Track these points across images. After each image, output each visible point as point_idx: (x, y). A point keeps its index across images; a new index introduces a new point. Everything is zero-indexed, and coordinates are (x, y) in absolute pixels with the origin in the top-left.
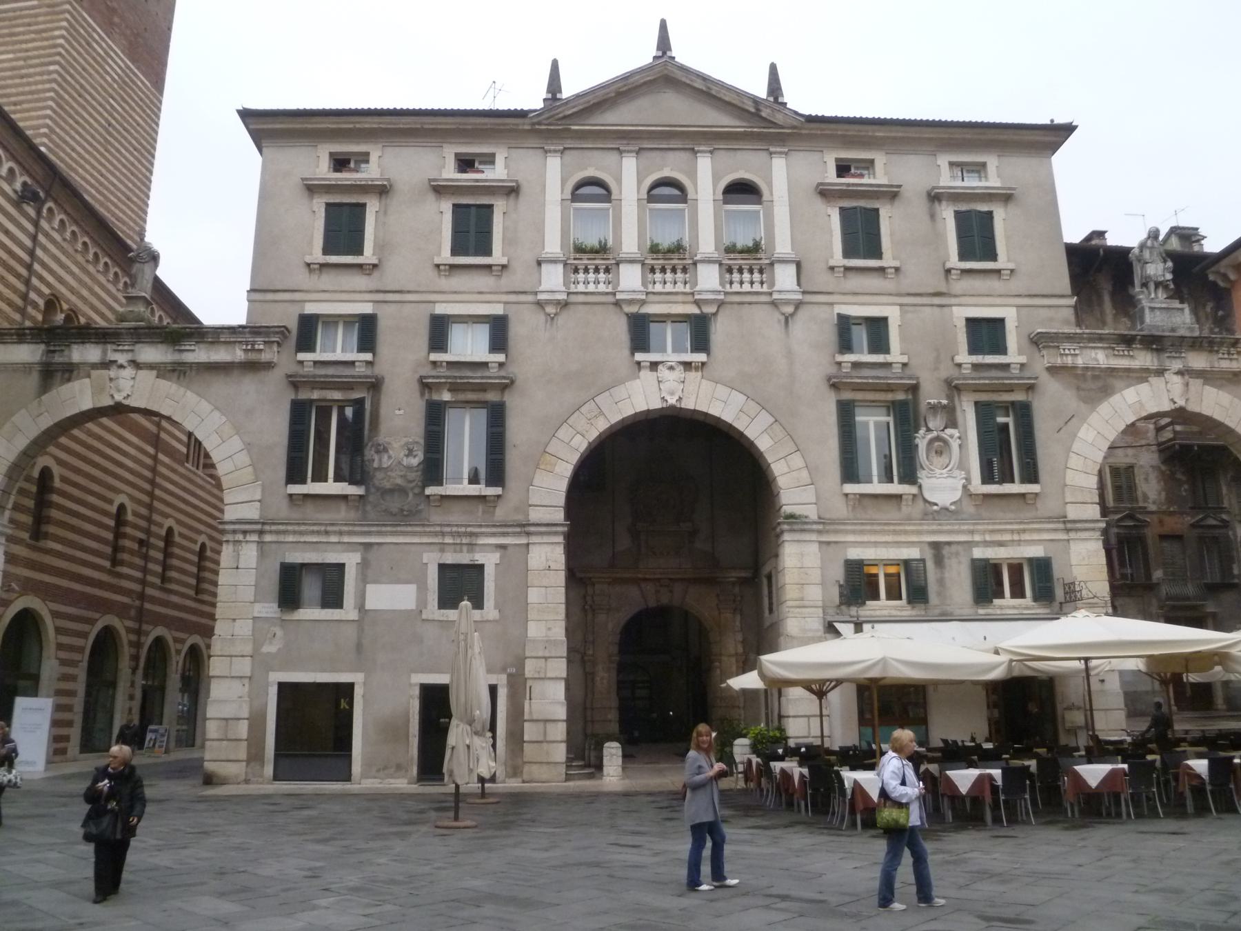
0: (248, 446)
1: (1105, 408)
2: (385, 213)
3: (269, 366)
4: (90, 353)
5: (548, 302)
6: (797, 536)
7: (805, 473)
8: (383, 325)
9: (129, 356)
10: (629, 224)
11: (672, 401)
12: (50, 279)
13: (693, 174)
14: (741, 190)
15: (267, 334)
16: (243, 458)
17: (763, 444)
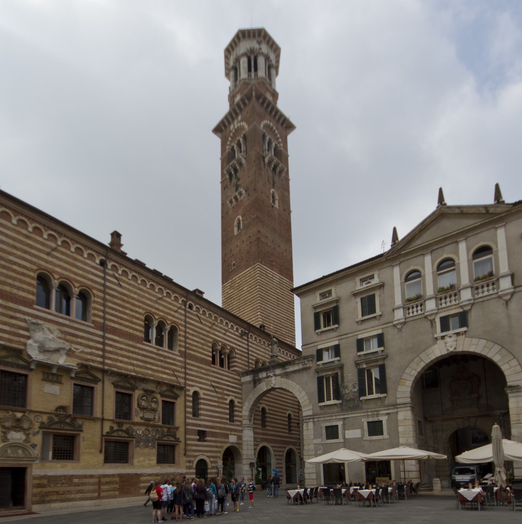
4: (263, 375)
9: (273, 373)
12: (255, 355)
17: (496, 359)
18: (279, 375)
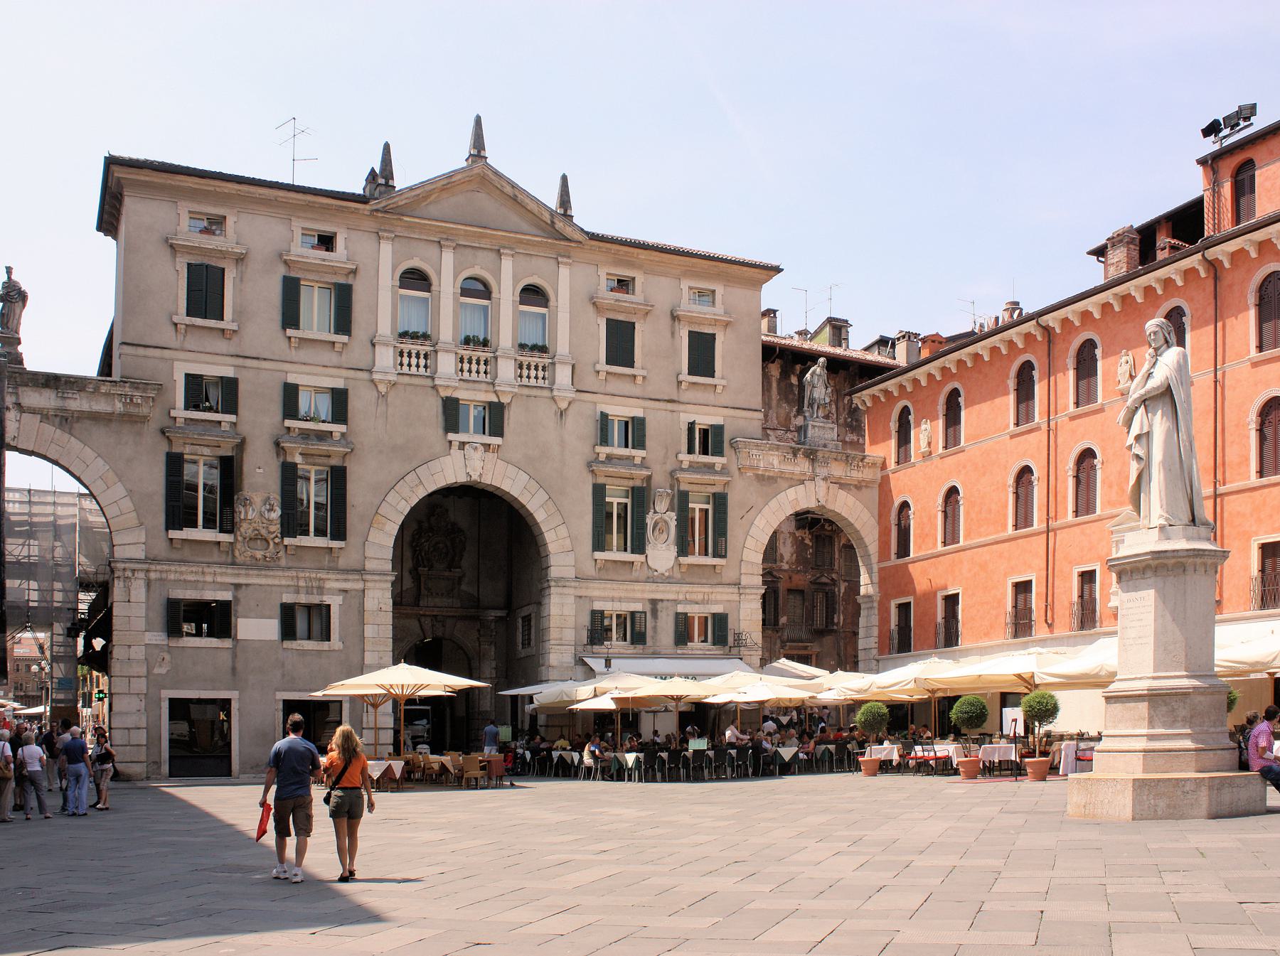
0: (130, 493)
1: (773, 503)
2: (241, 280)
3: (144, 419)
5: (381, 381)
6: (560, 590)
7: (568, 541)
8: (242, 387)
10: (448, 314)
11: (475, 477)
13: (497, 273)
14: (533, 294)
15: (145, 391)
16: (127, 504)
17: (540, 516)
18: (33, 411)
